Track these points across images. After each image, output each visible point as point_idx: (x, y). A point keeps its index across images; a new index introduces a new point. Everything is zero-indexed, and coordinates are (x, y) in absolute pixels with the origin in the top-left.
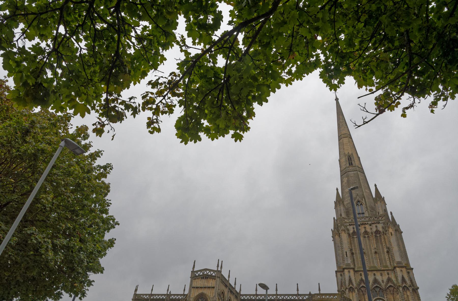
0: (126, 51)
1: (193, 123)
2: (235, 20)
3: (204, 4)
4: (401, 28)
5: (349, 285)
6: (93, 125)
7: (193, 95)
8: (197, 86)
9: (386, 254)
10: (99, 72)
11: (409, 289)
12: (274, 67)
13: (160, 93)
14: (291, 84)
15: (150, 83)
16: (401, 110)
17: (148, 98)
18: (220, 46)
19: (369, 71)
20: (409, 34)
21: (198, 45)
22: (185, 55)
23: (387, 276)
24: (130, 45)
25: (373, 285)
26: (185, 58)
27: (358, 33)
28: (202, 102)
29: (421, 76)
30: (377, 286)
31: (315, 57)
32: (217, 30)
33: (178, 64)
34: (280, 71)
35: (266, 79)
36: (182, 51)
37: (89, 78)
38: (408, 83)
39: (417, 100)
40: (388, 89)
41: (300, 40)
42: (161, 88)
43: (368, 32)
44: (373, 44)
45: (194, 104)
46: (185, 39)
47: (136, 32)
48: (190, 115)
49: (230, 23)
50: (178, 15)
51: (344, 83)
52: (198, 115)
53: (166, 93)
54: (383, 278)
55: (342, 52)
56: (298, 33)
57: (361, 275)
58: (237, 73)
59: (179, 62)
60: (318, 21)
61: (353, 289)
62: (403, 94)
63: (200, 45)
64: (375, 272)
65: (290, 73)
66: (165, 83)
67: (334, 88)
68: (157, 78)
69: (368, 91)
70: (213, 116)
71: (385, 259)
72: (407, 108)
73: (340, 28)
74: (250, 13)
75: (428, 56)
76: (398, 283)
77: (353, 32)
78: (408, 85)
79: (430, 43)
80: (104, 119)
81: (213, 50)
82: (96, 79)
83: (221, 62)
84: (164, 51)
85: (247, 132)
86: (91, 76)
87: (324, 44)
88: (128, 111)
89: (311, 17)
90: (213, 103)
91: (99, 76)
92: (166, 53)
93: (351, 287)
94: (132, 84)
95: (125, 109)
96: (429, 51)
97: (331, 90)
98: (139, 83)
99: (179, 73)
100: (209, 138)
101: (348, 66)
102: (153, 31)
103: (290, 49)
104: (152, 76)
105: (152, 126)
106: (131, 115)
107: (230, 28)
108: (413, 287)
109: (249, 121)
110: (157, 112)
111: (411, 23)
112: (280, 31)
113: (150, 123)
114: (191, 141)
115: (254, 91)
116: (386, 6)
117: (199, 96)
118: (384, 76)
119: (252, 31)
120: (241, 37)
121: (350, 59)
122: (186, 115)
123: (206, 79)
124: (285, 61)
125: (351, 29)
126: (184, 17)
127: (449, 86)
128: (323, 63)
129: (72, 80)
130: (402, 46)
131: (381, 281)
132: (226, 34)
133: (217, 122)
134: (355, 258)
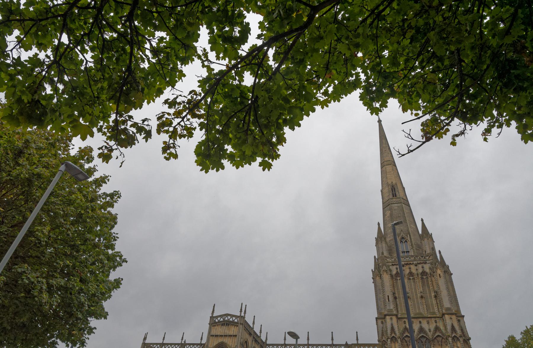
0: (139, 66)
1: (215, 148)
2: (264, 32)
3: (230, 13)
4: (451, 46)
5: (391, 335)
6: (99, 149)
7: (216, 117)
8: (221, 106)
9: (433, 299)
10: (107, 89)
11: (459, 340)
12: (308, 87)
13: (178, 114)
14: (327, 106)
15: (166, 102)
16: (451, 137)
17: (164, 119)
18: (248, 62)
19: (415, 94)
20: (461, 53)
21: (222, 60)
22: (207, 71)
23: (435, 324)
24: (144, 58)
26: (207, 74)
27: (404, 50)
28: (226, 125)
29: (473, 100)
30: (423, 336)
31: (354, 76)
32: (244, 44)
33: (199, 81)
34: (315, 91)
35: (299, 100)
36: (203, 66)
37: (96, 96)
38: (458, 107)
39: (468, 127)
40: (435, 114)
41: (338, 57)
42: (180, 108)
43: (414, 50)
44: (420, 63)
45: (218, 127)
46: (207, 53)
47: (151, 45)
48: (212, 140)
49: (259, 37)
50: (201, 27)
51: (386, 107)
52: (221, 140)
53: (184, 114)
54: (430, 326)
55: (385, 71)
56: (336, 49)
57: (405, 322)
58: (266, 93)
59: (201, 79)
60: (358, 37)
61: (396, 338)
62: (453, 120)
63: (225, 60)
64: (421, 320)
65: (326, 93)
66: (184, 102)
67: (375, 111)
68: (175, 96)
69: (413, 115)
70: (238, 141)
71: (432, 304)
72: (457, 135)
73: (383, 43)
74: (282, 26)
75: (481, 78)
76: (447, 332)
77: (397, 49)
78: (459, 110)
79: (483, 63)
80: (112, 143)
81: (239, 66)
82: (104, 97)
83: (248, 80)
84: (183, 66)
85: (276, 159)
86: (98, 93)
87: (365, 62)
88: (141, 135)
89: (350, 32)
90: (238, 126)
91: (107, 93)
92: (185, 69)
93: (393, 337)
94: (145, 104)
95: (137, 133)
96: (483, 72)
97: (372, 114)
98: (154, 101)
99: (201, 91)
100: (233, 166)
101: (391, 87)
102: (170, 43)
103: (327, 67)
104: (168, 93)
105: (168, 151)
106: (143, 138)
107: (259, 43)
108: (464, 338)
109: (279, 147)
110: (174, 135)
111: (462, 41)
112: (316, 47)
113: (166, 148)
114: (213, 169)
115: (285, 114)
116: (435, 22)
117: (223, 118)
118: (432, 99)
119: (283, 46)
120: (271, 52)
121: (394, 79)
122: (207, 140)
123: (231, 99)
124: (321, 80)
125: (396, 45)
126: (207, 28)
127: (504, 112)
128: (363, 84)
129: (75, 98)
130: (452, 66)
131: (428, 331)
132: (254, 49)
133: (243, 148)
134: (398, 303)
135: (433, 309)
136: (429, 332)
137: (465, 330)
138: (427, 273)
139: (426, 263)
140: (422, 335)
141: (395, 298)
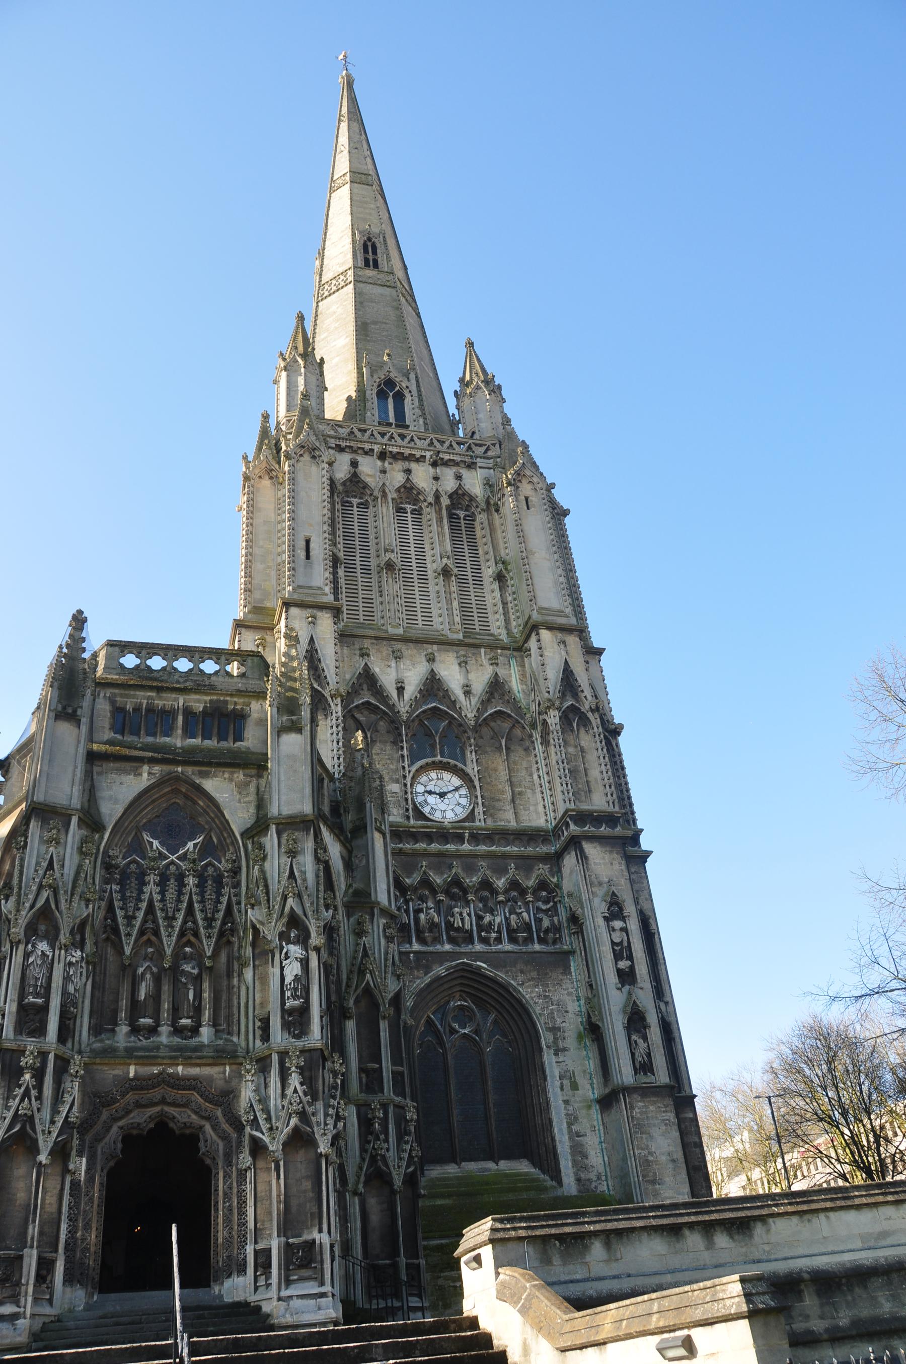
25: (416, 703)
54: (472, 676)
71: (482, 609)
134: (342, 582)
135: (485, 621)
136: (462, 697)
137: (601, 694)
138: (472, 499)
139: (471, 466)
140: (434, 704)
141: (336, 561)
